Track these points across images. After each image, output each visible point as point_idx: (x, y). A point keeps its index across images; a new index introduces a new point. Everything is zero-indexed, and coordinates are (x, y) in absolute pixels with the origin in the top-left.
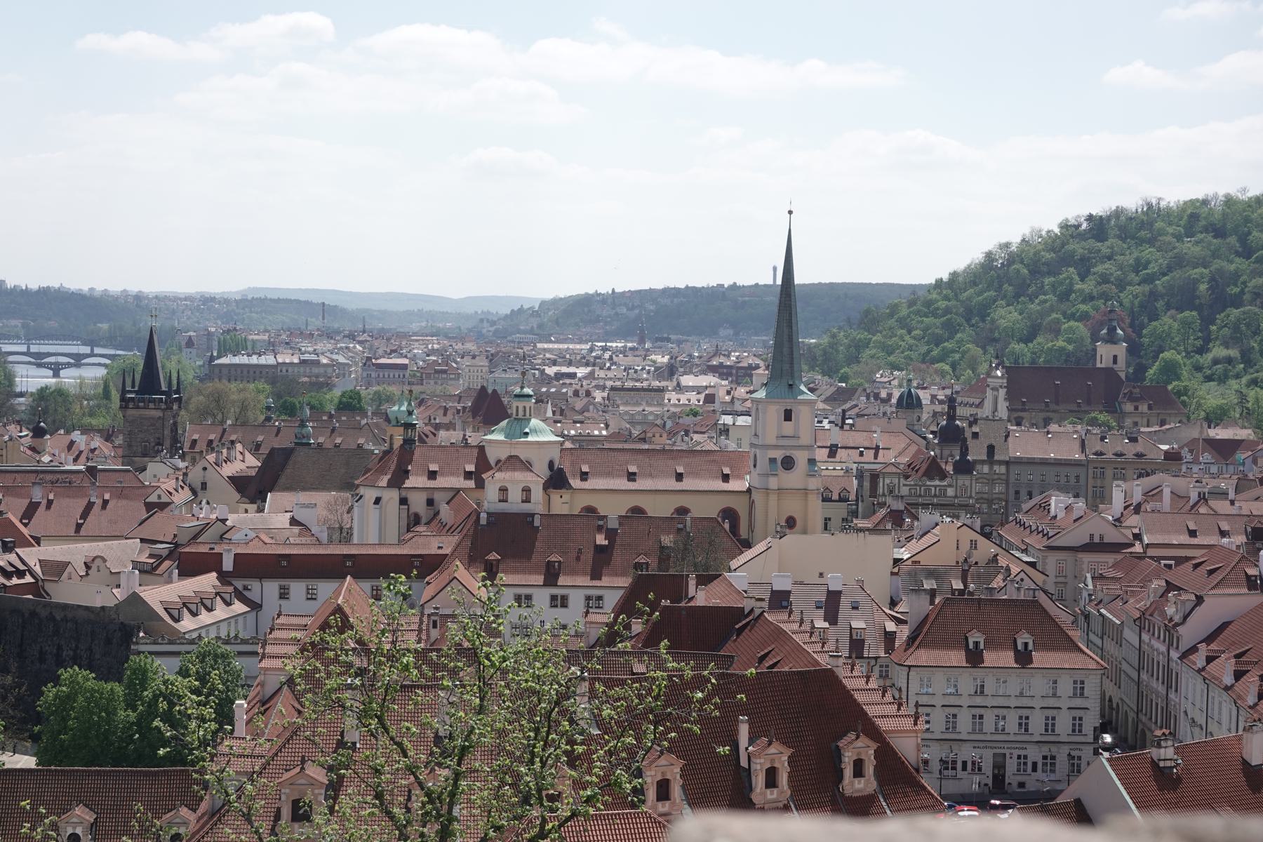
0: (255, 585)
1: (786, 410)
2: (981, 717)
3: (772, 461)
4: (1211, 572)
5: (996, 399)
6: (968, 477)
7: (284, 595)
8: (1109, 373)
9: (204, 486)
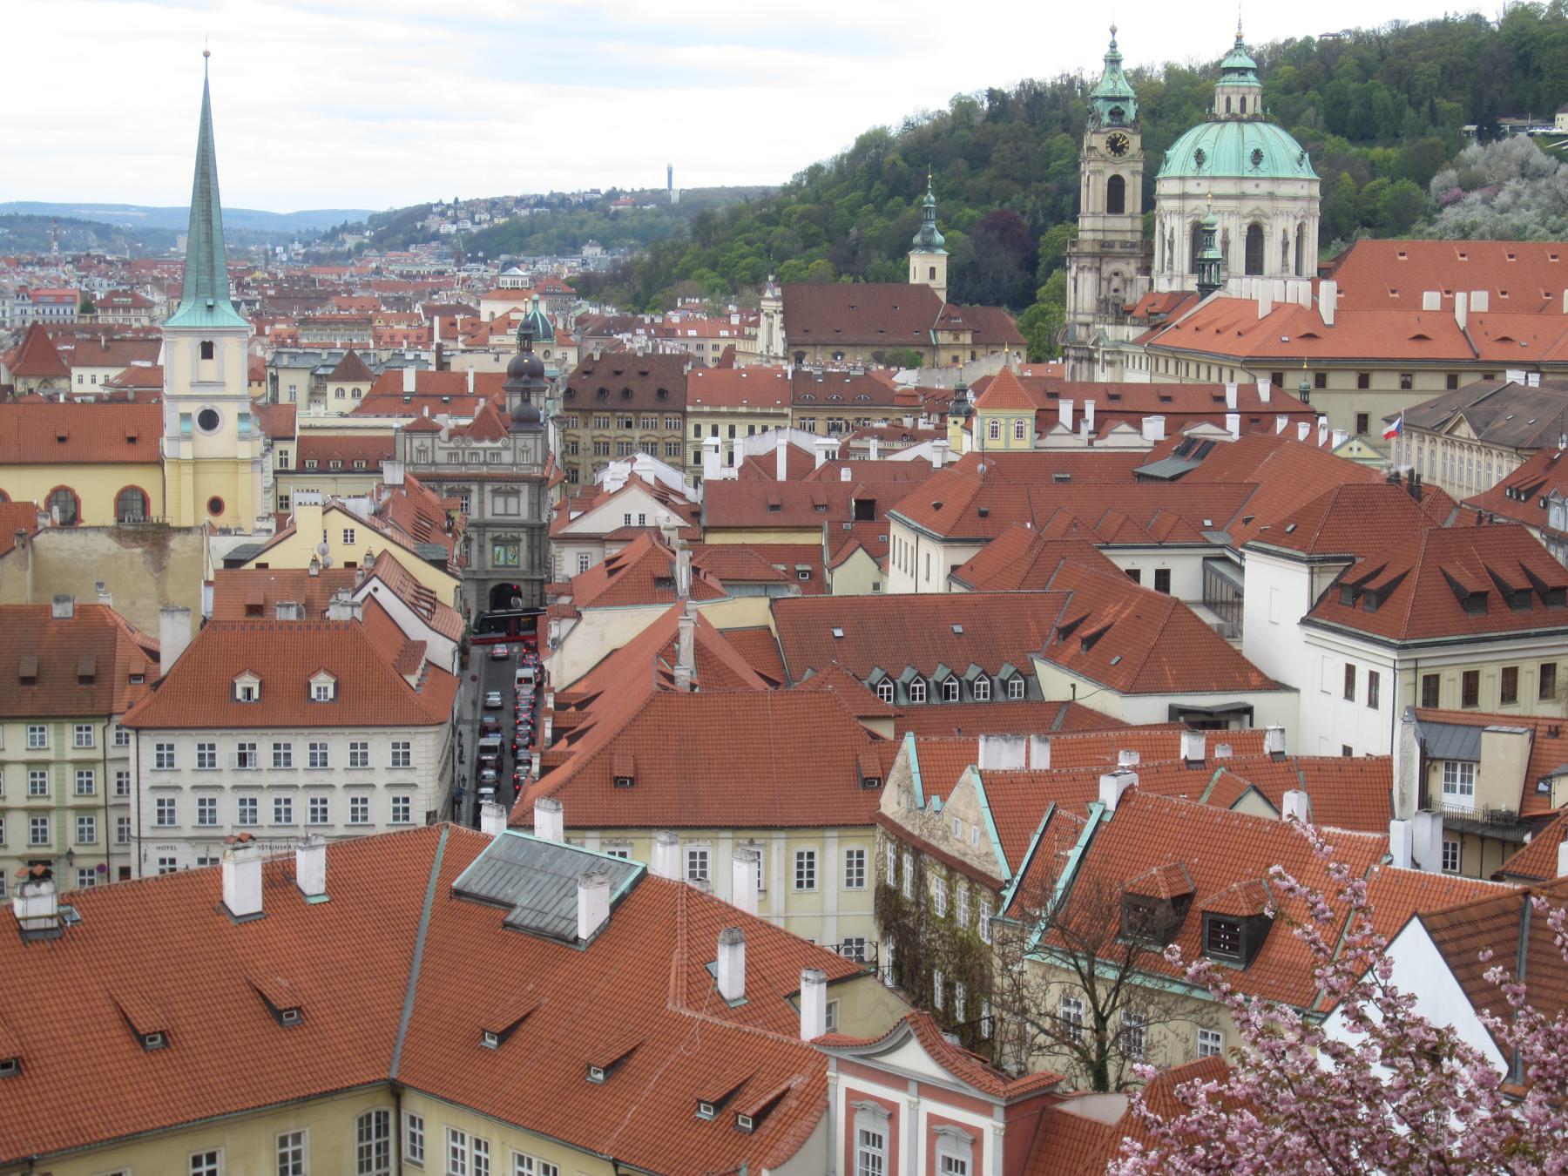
1: (204, 344)
2: (253, 802)
3: (186, 417)
5: (771, 326)
6: (532, 436)
8: (924, 288)
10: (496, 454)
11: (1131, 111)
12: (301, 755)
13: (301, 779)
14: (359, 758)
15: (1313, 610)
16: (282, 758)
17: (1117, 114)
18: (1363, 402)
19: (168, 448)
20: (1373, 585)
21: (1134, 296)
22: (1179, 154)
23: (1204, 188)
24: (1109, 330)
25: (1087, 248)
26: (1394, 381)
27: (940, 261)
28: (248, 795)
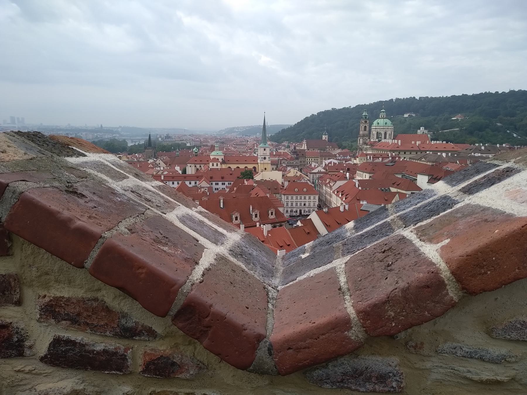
0: (168, 182)
3: (262, 158)
4: (338, 177)
7: (173, 183)
9: (159, 164)
11: (367, 117)
12: (303, 198)
13: (303, 201)
14: (310, 198)
15: (428, 181)
16: (301, 199)
17: (366, 118)
18: (405, 156)
19: (259, 161)
20: (438, 178)
21: (368, 141)
22: (375, 123)
23: (379, 127)
24: (365, 146)
25: (361, 135)
26: (409, 153)
27: (327, 137)
28: (297, 202)
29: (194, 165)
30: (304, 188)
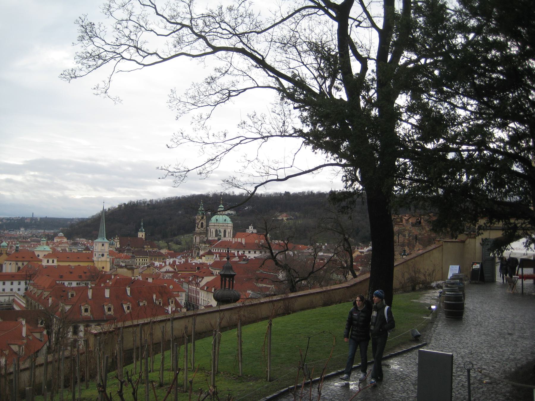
3: (100, 255)
4: (204, 273)
10: (129, 262)
29: (15, 263)
30: (170, 285)
